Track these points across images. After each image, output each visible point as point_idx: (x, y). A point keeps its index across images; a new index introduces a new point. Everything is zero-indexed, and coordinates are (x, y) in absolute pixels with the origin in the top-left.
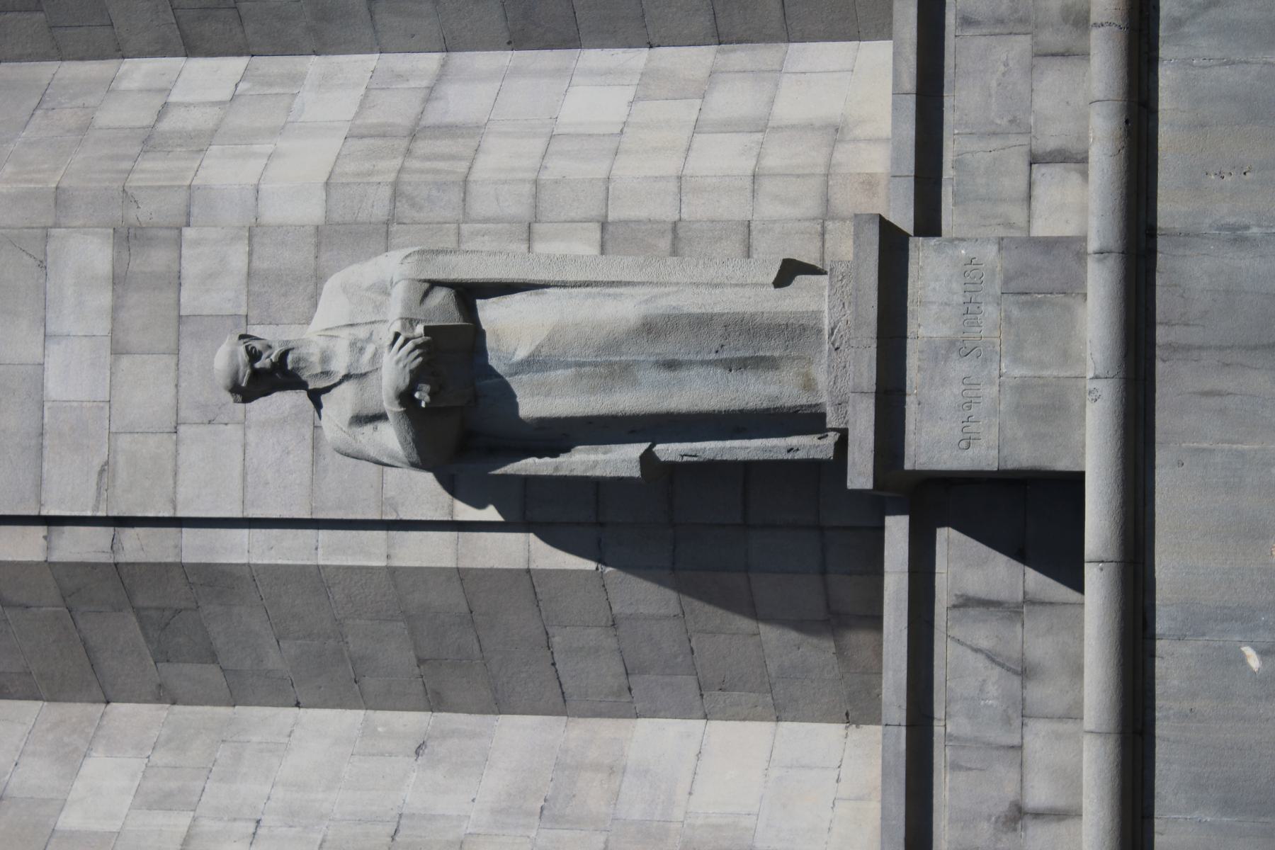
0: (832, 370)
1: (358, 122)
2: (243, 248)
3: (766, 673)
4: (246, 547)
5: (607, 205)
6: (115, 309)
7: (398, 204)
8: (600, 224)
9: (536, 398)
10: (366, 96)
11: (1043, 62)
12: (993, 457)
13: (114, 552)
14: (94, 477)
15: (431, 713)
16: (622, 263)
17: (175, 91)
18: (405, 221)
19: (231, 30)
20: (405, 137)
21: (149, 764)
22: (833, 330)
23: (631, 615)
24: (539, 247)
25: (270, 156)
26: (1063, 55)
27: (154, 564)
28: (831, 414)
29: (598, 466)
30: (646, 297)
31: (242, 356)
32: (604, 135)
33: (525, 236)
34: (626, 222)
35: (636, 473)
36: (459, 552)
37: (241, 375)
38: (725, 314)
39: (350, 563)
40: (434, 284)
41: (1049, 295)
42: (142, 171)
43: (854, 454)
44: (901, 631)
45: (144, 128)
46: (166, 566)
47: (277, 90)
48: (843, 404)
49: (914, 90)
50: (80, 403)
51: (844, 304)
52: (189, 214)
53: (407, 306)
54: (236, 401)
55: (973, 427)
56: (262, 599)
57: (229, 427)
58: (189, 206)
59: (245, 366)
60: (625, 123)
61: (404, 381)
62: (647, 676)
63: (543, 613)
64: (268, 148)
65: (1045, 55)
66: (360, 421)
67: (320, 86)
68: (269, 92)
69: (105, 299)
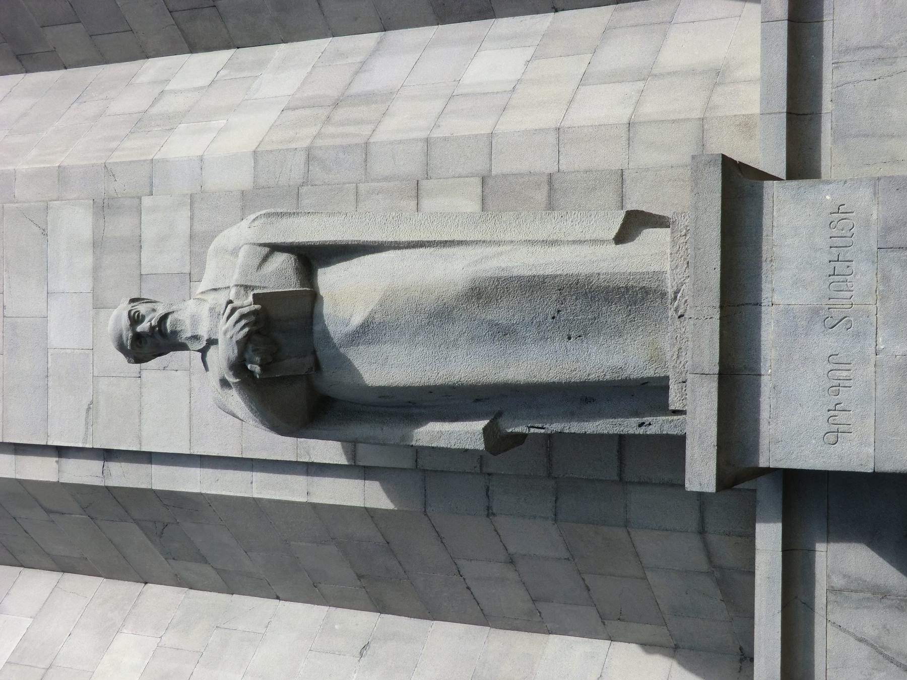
2: (185, 213)
6: (96, 269)
7: (310, 167)
9: (373, 367)
10: (310, 73)
14: (84, 413)
16: (457, 220)
20: (329, 106)
21: (160, 645)
22: (676, 293)
24: (428, 204)
29: (443, 437)
31: (125, 322)
33: (414, 193)
34: (505, 176)
35: (480, 445)
36: (366, 492)
37: (125, 339)
40: (275, 248)
43: (693, 448)
45: (139, 113)
49: (786, 16)
50: (73, 350)
51: (688, 263)
52: (151, 185)
55: (842, 417)
57: (179, 373)
58: (151, 177)
64: (222, 123)
67: (279, 67)
69: (87, 261)
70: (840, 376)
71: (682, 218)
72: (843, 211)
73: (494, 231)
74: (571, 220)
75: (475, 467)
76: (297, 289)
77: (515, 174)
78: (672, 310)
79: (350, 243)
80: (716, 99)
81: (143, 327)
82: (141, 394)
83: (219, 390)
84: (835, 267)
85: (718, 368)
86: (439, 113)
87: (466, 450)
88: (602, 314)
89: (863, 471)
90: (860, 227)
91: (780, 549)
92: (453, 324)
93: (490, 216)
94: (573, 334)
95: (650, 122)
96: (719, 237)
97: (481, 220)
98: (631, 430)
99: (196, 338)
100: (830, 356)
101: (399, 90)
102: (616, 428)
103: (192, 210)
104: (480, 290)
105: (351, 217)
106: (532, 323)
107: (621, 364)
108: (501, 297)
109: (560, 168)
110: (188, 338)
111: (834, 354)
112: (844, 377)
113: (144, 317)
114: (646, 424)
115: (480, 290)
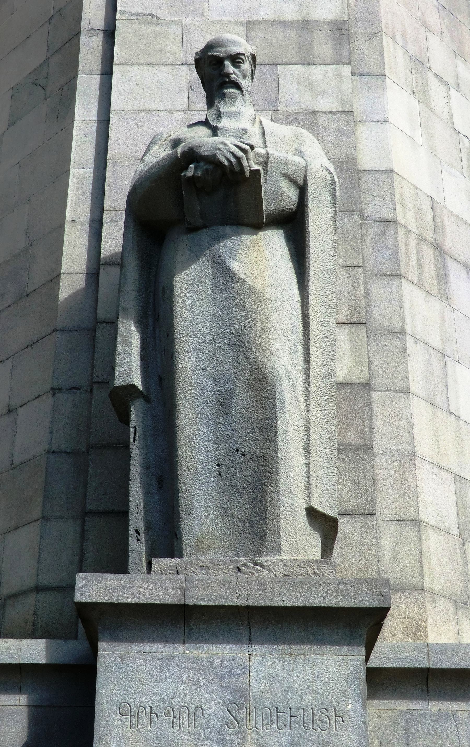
2: (335, 106)
4: (86, 119)
5: (385, 391)
6: (283, 23)
8: (367, 382)
13: (89, 30)
14: (148, 12)
16: (328, 360)
18: (364, 229)
20: (435, 241)
24: (344, 332)
29: (126, 347)
31: (235, 50)
33: (354, 320)
34: (370, 405)
35: (118, 382)
38: (277, 454)
39: (69, 193)
43: (116, 580)
51: (289, 576)
52: (362, 74)
53: (279, 161)
55: (145, 719)
56: (48, 140)
57: (186, 100)
58: (368, 74)
59: (226, 52)
60: (459, 417)
63: (22, 352)
70: (183, 718)
71: (330, 570)
72: (337, 720)
73: (318, 394)
74: (329, 466)
75: (98, 377)
76: (264, 211)
77: (371, 414)
78: (245, 561)
79: (307, 260)
80: (442, 602)
81: (229, 67)
82: (166, 64)
83: (170, 138)
84: (284, 713)
85: (190, 604)
86: (429, 343)
87: (114, 369)
88: (240, 495)
89: (95, 739)
90: (322, 736)
91: (21, 662)
92: (232, 356)
93: (332, 390)
94: (222, 468)
95: (420, 541)
96: (313, 605)
97: (328, 382)
98: (133, 523)
99: (219, 116)
100: (202, 709)
101: (450, 306)
102: (134, 508)
103: (338, 112)
104: (264, 381)
105: (332, 261)
106: (233, 430)
107: (195, 513)
108: (257, 401)
109: (377, 456)
110: (218, 109)
111: (204, 712)
112: (183, 721)
113: (238, 67)
114: (138, 536)
115: (264, 381)
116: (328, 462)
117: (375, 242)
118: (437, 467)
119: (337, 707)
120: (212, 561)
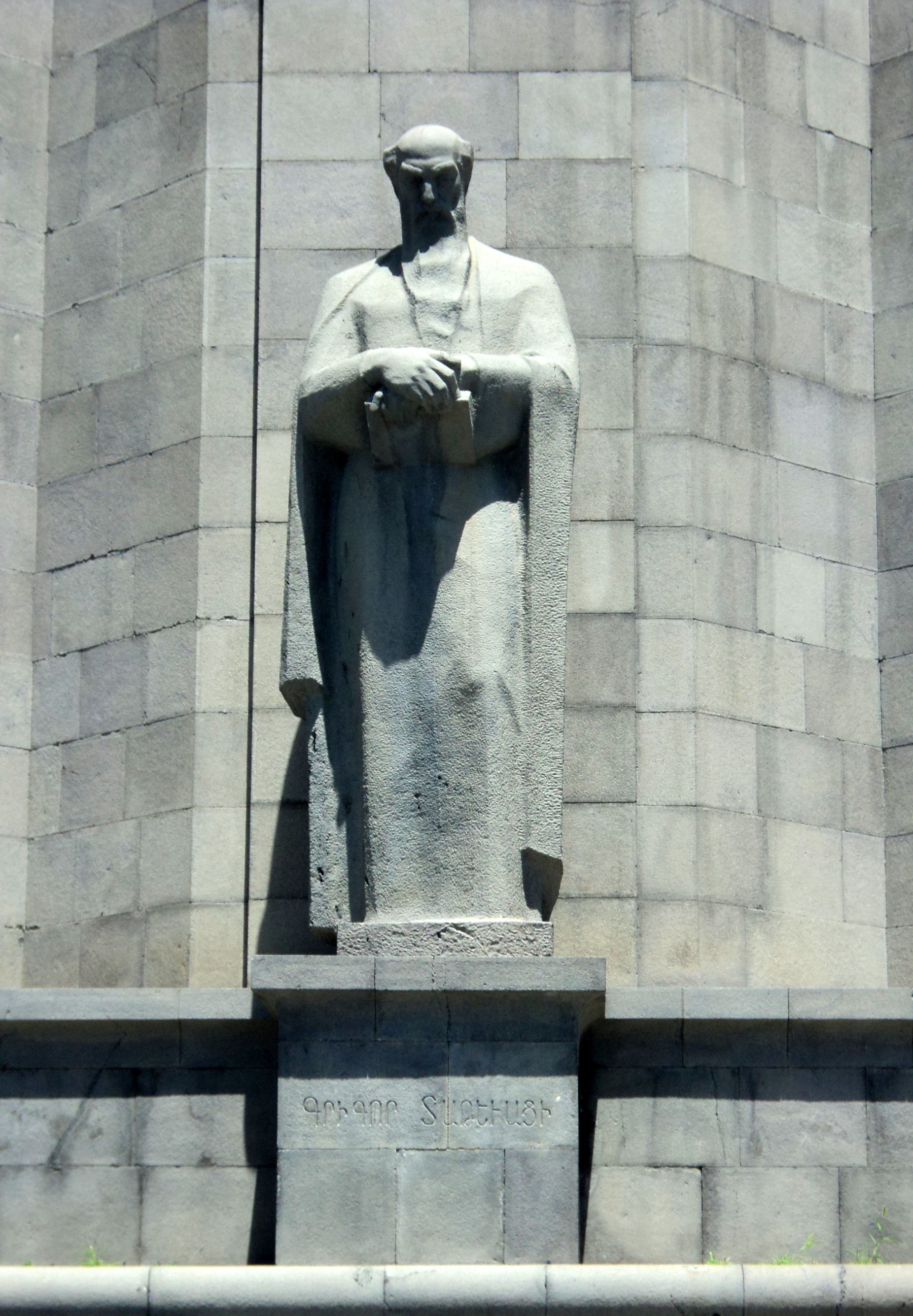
0: (412, 929)
1: (776, 293)
3: (82, 826)
4: (225, 166)
7: (662, 348)
10: (812, 301)
11: (834, 1181)
12: (294, 1142)
15: (40, 400)
16: (555, 652)
17: (822, 53)
18: (640, 360)
19: (902, 122)
20: (754, 354)
22: (463, 929)
23: (147, 657)
25: (728, 181)
26: (840, 1206)
27: (205, 48)
28: (355, 929)
30: (508, 685)
32: (755, 609)
33: (618, 515)
36: (220, 438)
39: (206, 299)
41: (501, 1211)
42: (707, 18)
43: (296, 963)
44: (104, 1010)
45: (769, 15)
46: (202, 65)
47: (822, 183)
48: (368, 945)
52: (650, 79)
54: (387, 155)
55: (333, 1114)
57: (377, 141)
61: (395, 377)
62: (79, 675)
63: (149, 546)
64: (741, 178)
65: (840, 1185)
66: (358, 317)
68: (819, 173)
72: (545, 1114)
74: (553, 794)
103: (610, 161)
116: (551, 789)
117: (656, 379)
118: (731, 721)
119: (544, 1099)
120: (408, 926)
